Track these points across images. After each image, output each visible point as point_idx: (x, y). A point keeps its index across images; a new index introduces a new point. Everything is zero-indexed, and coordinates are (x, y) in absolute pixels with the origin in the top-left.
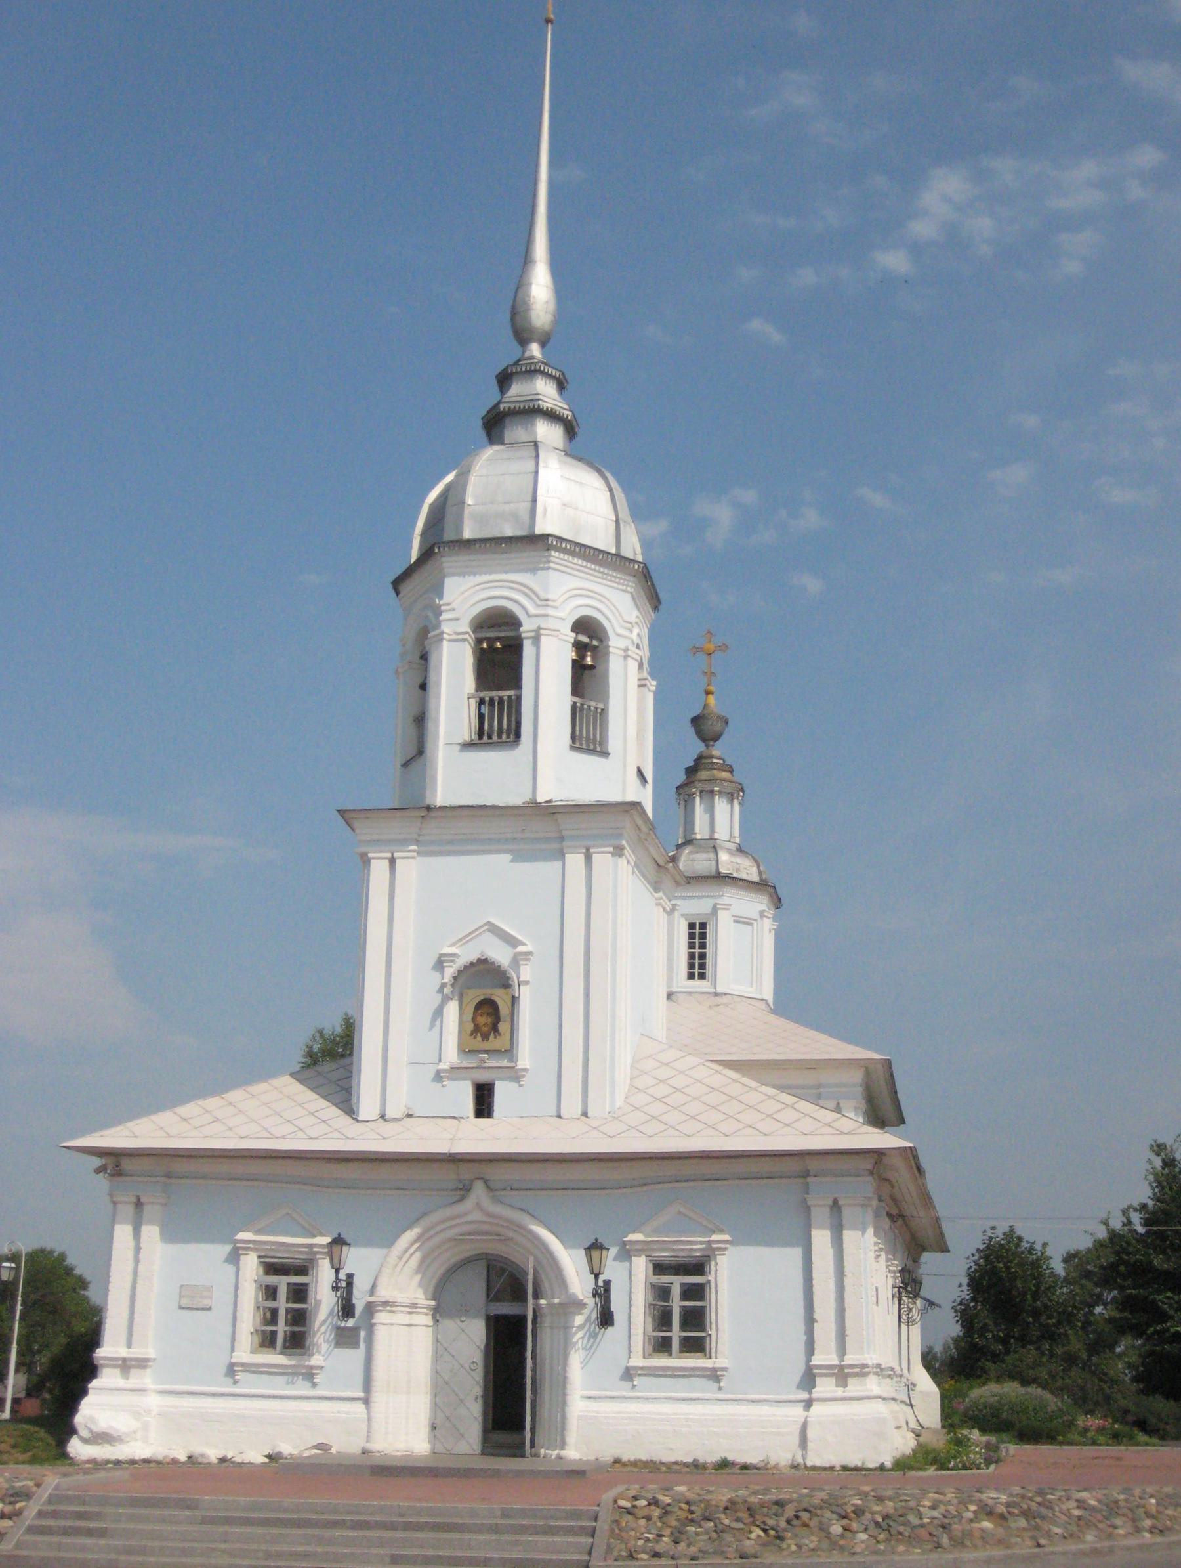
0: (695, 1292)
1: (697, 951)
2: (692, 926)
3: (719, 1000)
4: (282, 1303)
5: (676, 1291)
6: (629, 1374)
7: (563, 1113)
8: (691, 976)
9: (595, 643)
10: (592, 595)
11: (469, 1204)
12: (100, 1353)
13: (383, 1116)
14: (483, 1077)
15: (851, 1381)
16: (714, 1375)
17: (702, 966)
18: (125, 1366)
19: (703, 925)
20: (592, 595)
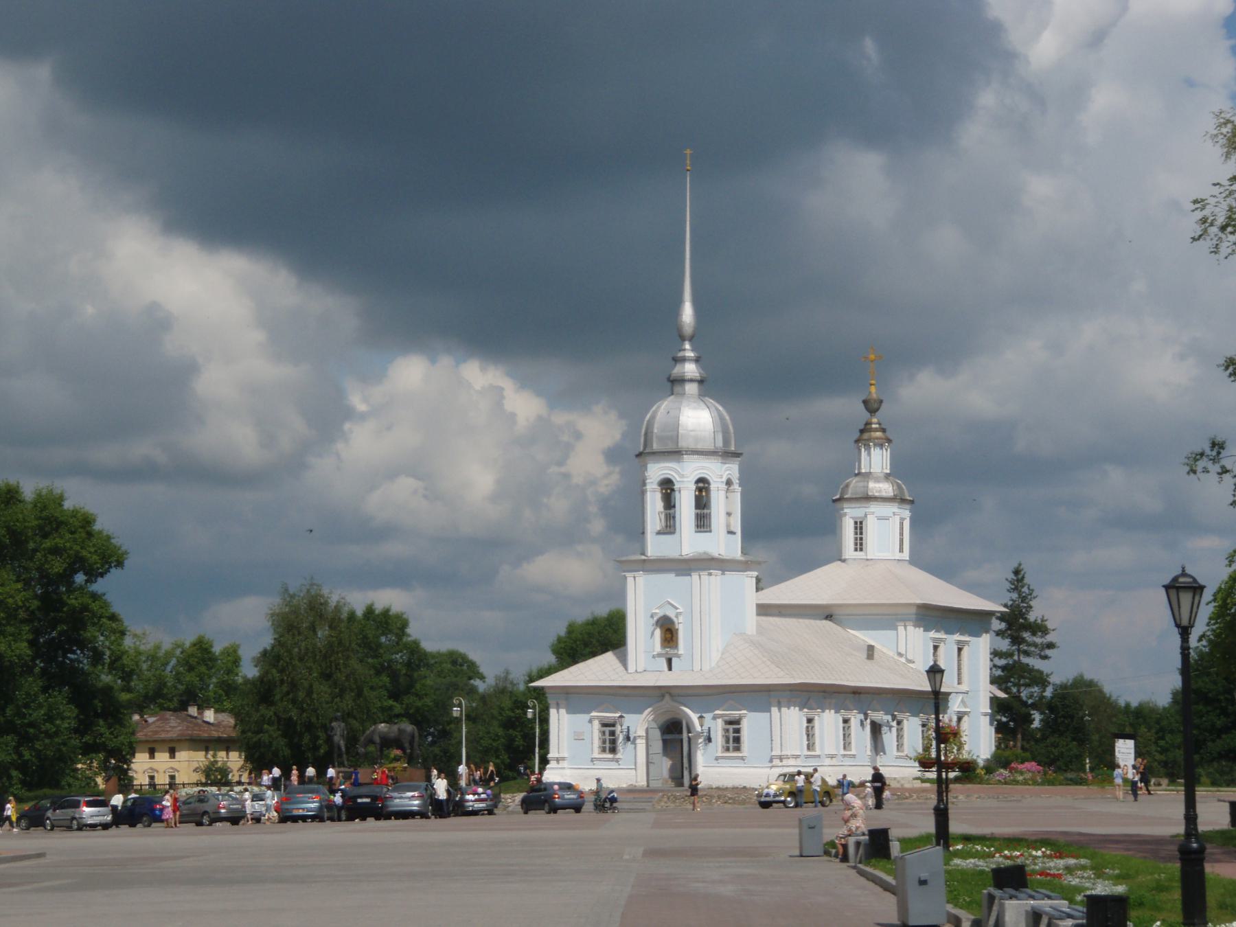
0: (738, 731)
1: (859, 536)
2: (856, 523)
3: (868, 562)
4: (607, 737)
5: (731, 731)
6: (717, 759)
7: (694, 669)
8: (856, 550)
9: (706, 485)
10: (703, 468)
11: (664, 702)
12: (550, 756)
13: (636, 671)
14: (668, 656)
15: (784, 760)
16: (742, 758)
17: (861, 544)
18: (558, 760)
19: (861, 523)
20: (703, 468)
